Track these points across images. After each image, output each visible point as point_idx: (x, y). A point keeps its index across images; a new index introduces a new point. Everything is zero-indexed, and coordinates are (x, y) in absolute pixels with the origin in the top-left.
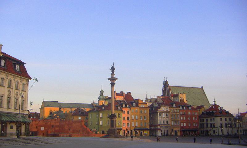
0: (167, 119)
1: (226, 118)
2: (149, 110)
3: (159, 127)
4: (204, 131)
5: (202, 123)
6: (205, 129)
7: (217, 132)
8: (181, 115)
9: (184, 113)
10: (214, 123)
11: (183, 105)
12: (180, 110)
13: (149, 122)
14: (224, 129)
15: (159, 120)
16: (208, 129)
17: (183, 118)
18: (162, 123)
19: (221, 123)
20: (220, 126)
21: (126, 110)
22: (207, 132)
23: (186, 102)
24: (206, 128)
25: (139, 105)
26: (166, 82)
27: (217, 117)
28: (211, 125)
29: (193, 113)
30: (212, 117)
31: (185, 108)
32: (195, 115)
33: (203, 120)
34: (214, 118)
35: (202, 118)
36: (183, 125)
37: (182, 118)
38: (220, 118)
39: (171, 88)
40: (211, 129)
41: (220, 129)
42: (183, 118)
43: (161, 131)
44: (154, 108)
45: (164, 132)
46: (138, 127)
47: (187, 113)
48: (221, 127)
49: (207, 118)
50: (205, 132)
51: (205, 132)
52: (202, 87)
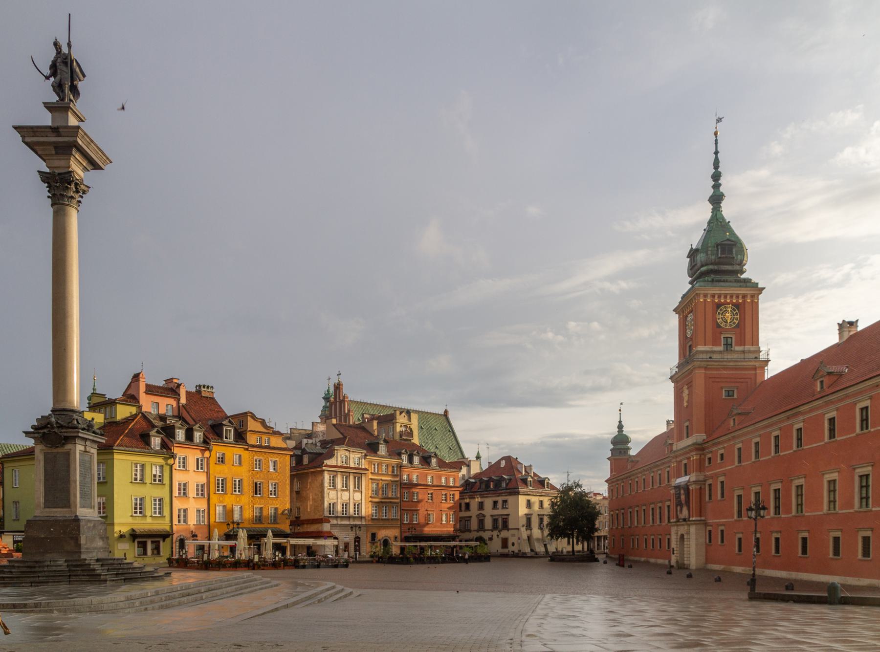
0: (357, 496)
1: (541, 498)
2: (288, 458)
10: (508, 515)
14: (536, 533)
15: (326, 499)
16: (486, 535)
21: (192, 455)
23: (416, 440)
24: (478, 531)
28: (495, 521)
30: (500, 495)
31: (416, 460)
40: (495, 533)
41: (524, 533)
48: (529, 526)
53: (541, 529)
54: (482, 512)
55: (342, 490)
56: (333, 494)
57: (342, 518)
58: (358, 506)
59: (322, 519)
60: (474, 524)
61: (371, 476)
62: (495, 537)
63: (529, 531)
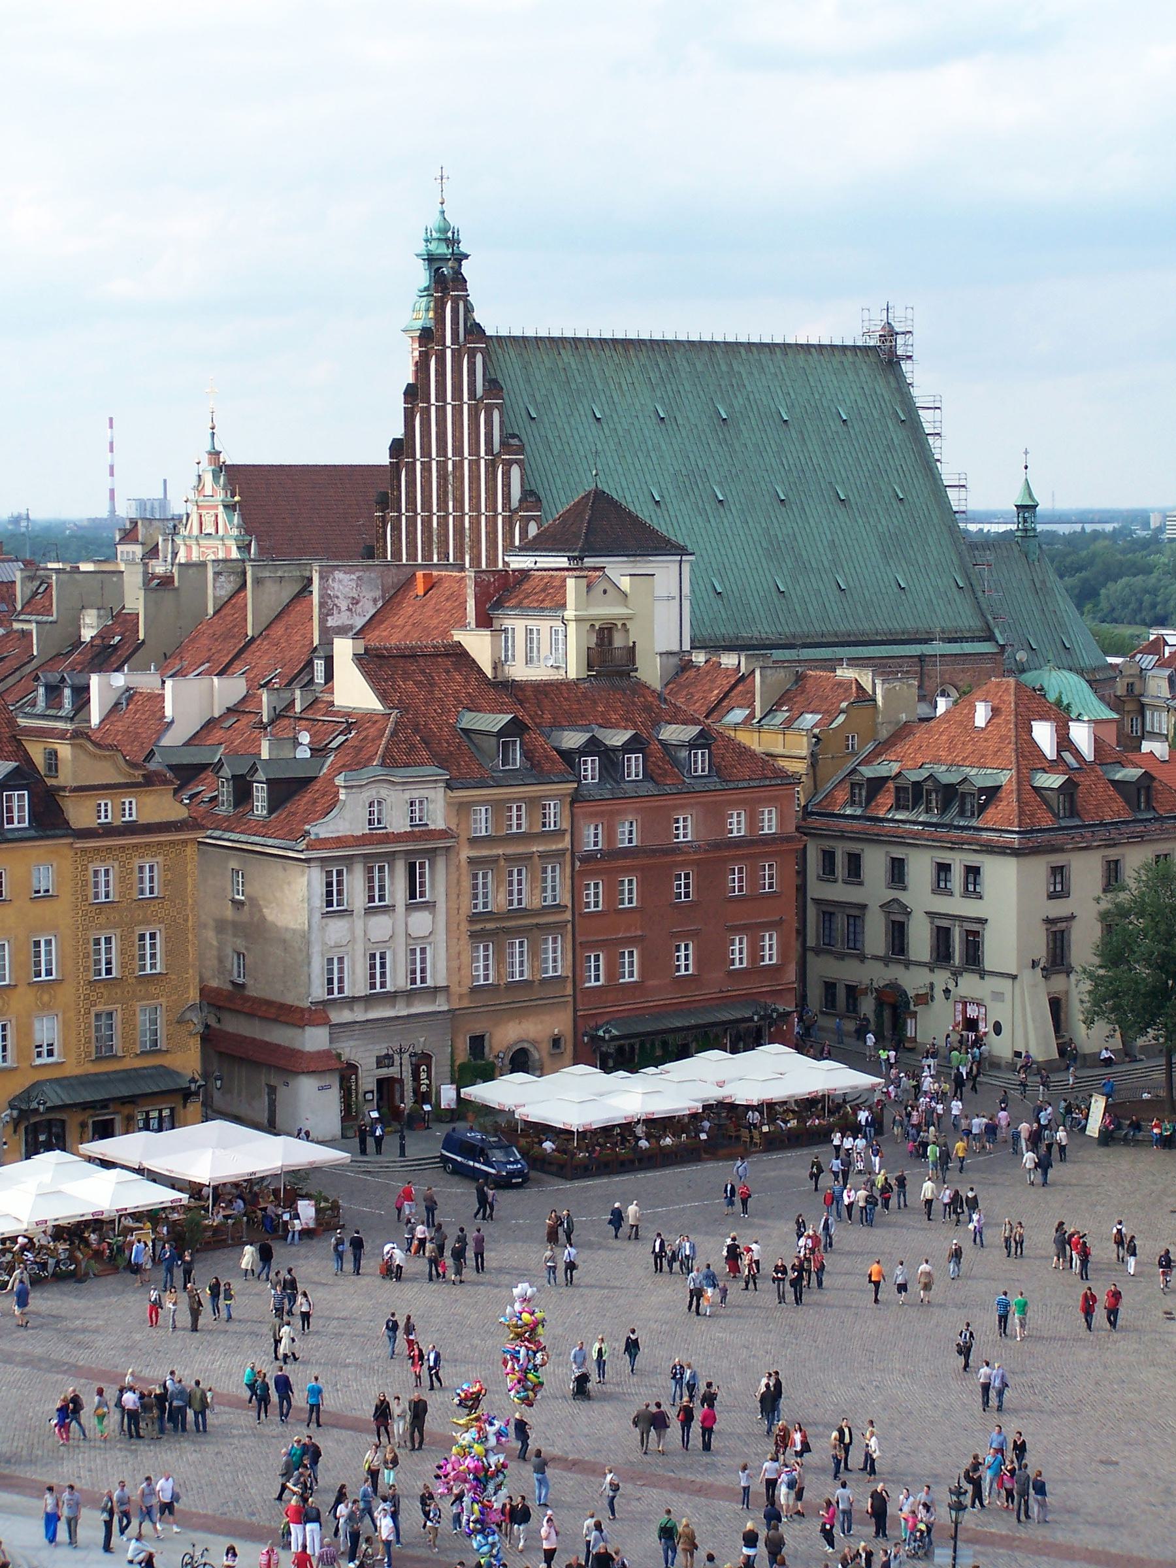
0: (421, 922)
1: (1113, 853)
2: (190, 850)
3: (315, 1039)
4: (853, 992)
5: (839, 892)
6: (875, 974)
7: (998, 1028)
8: (587, 865)
9: (628, 833)
10: (983, 921)
11: (617, 738)
12: (576, 799)
13: (193, 995)
15: (316, 949)
16: (913, 981)
17: (613, 893)
18: (356, 983)
19: (1049, 921)
20: (1040, 951)
22: (895, 1009)
24: (886, 961)
25: (80, 814)
26: (446, 277)
27: (1016, 853)
28: (942, 936)
29: (737, 826)
32: (754, 847)
33: (855, 861)
34: (974, 860)
35: (842, 837)
36: (614, 971)
37: (594, 897)
38: (1040, 866)
39: (510, 369)
40: (941, 978)
42: (613, 893)
43: (347, 1073)
44: (260, 793)
45: (386, 1086)
46: (78, 1071)
47: (658, 819)
49: (898, 853)
50: (867, 1006)
51: (867, 1006)
52: (890, 333)
54: (903, 897)
55: (370, 911)
56: (337, 929)
57: (369, 1000)
58: (417, 950)
59: (302, 1010)
60: (875, 937)
61: (466, 853)
62: (938, 993)
63: (1059, 983)
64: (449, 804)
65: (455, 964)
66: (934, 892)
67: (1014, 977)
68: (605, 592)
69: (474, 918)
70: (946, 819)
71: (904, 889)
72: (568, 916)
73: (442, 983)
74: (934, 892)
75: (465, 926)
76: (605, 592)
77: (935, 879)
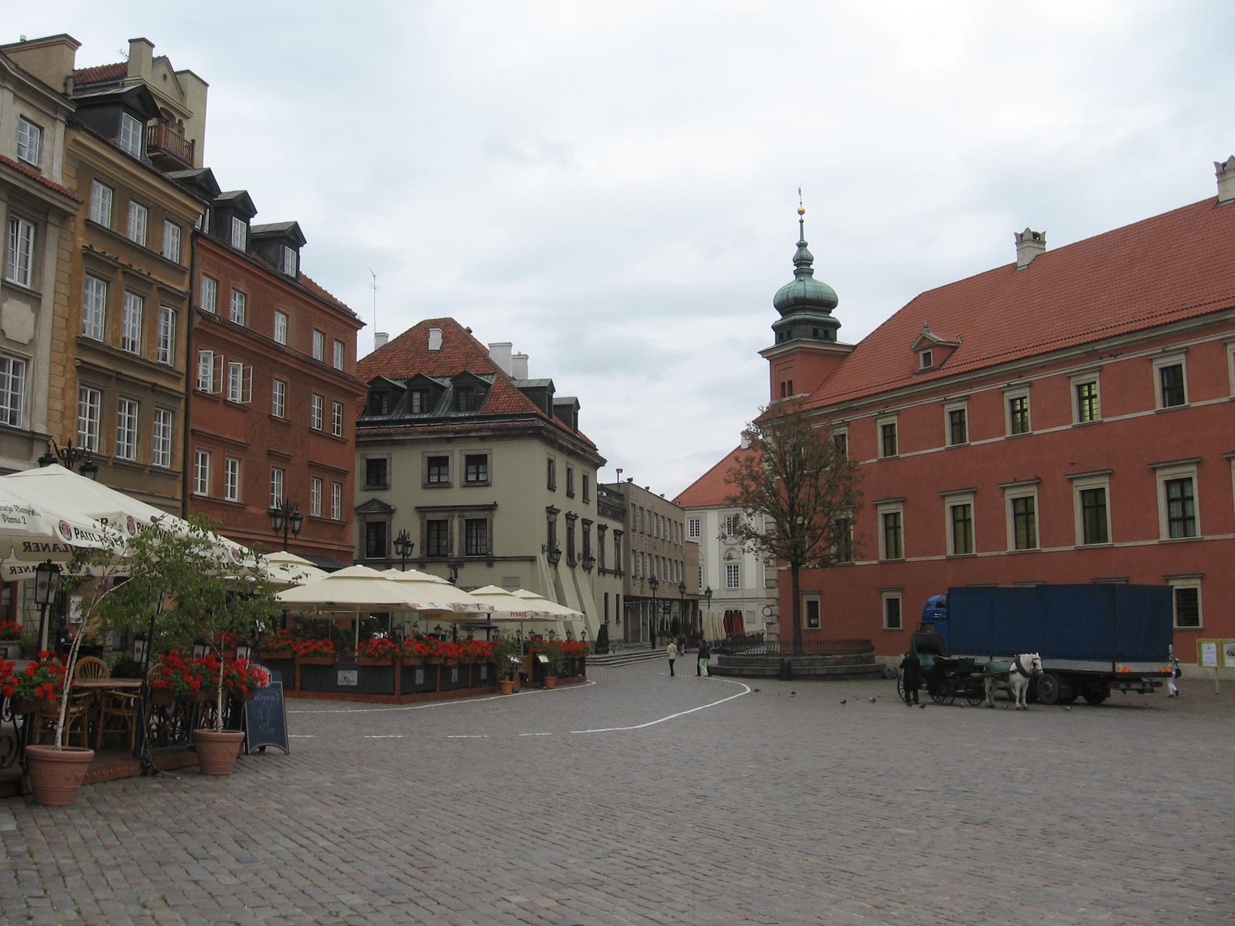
1: (570, 460)
10: (492, 508)
49: (376, 454)
53: (571, 564)
54: (383, 496)
64: (69, 154)
65: (58, 406)
66: (425, 487)
67: (532, 559)
68: (165, 77)
69: (84, 344)
70: (440, 413)
71: (386, 487)
72: (181, 388)
73: (41, 429)
74: (425, 487)
75: (73, 353)
76: (165, 77)
77: (426, 472)
